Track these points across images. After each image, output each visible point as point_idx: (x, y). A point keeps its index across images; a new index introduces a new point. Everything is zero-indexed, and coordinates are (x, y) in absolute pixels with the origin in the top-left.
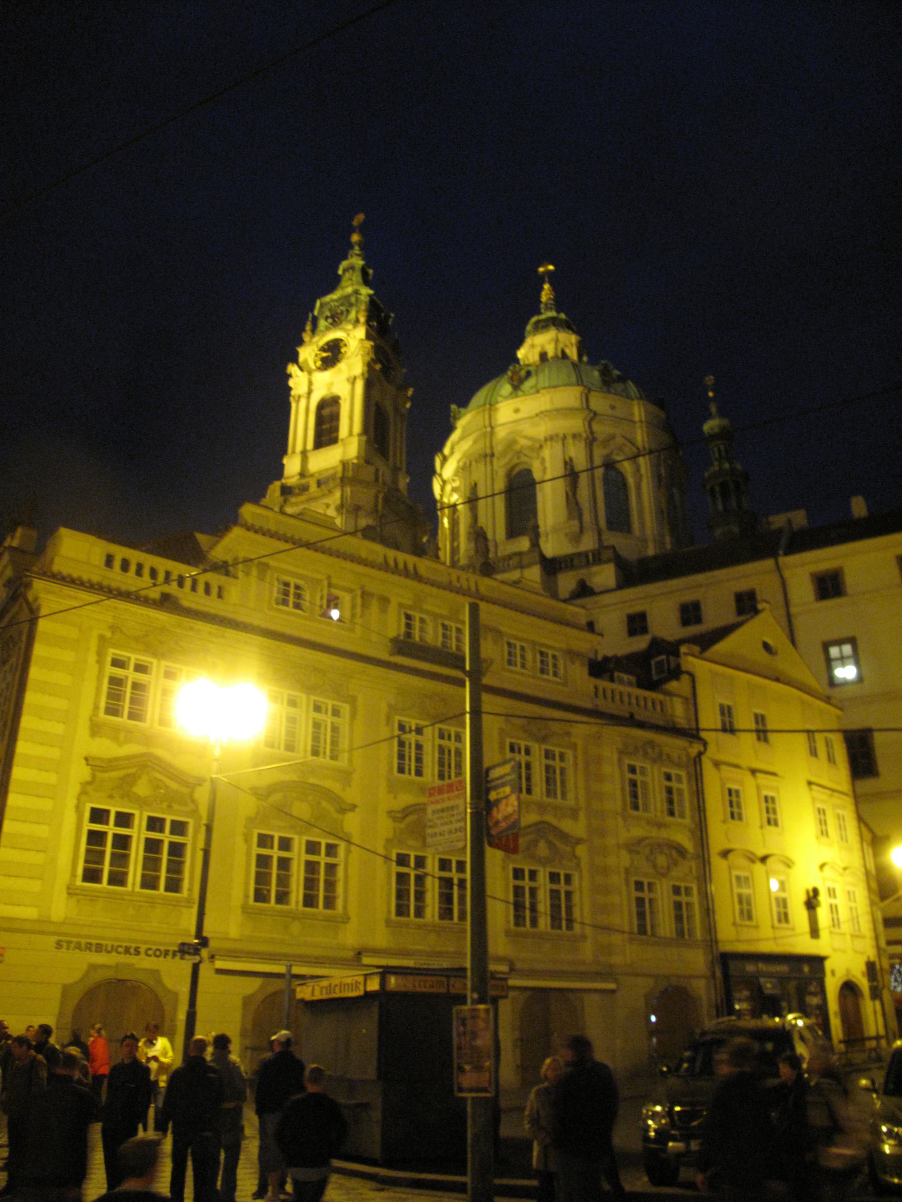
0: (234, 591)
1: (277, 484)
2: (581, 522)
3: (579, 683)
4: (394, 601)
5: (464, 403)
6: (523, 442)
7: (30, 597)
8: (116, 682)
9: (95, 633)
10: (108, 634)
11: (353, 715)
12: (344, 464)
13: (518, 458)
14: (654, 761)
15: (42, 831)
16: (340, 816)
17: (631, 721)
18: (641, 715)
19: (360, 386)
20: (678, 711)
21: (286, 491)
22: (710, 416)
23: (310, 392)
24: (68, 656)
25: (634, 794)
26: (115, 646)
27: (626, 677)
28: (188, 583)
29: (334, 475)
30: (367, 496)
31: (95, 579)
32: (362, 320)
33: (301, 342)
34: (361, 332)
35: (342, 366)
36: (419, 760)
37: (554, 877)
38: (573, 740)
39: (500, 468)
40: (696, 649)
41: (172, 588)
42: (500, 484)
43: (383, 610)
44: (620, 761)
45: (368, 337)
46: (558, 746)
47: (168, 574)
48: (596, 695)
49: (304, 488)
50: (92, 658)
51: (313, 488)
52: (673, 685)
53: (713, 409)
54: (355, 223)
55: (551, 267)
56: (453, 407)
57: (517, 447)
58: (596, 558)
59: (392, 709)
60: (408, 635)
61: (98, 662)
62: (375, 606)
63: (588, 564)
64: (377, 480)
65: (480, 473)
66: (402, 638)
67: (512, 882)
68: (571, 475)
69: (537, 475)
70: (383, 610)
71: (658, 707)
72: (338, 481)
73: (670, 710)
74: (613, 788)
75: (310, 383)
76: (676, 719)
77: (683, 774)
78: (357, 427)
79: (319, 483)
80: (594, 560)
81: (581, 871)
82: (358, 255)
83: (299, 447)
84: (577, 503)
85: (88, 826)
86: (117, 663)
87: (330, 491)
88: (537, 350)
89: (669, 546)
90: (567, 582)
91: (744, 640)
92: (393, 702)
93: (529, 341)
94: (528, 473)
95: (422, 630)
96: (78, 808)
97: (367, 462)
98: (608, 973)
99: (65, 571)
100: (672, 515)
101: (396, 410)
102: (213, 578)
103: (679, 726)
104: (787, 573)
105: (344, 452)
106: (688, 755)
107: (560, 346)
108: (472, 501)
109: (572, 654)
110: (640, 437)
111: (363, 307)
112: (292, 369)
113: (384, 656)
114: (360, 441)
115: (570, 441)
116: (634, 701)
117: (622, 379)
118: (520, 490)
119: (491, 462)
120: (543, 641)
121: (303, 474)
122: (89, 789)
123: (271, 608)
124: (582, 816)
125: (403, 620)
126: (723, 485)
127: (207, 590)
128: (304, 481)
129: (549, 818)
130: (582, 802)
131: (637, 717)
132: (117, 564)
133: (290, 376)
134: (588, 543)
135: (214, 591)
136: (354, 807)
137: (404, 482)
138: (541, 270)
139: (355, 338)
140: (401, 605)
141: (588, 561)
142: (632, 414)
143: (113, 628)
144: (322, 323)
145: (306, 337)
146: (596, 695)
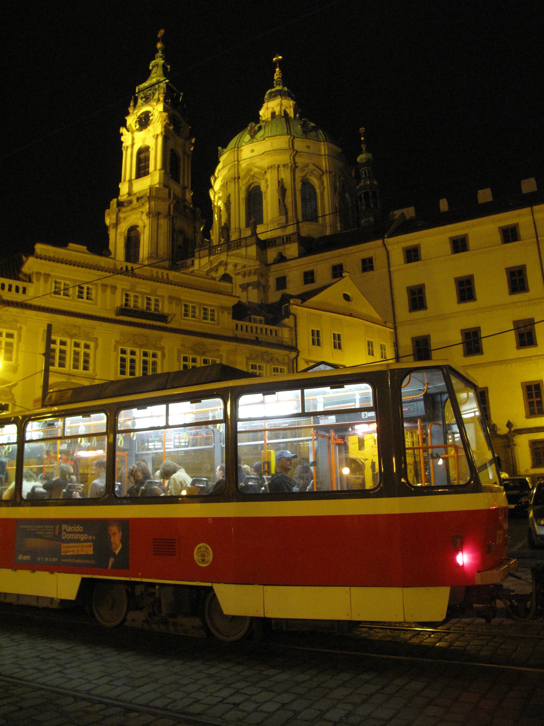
0: (32, 290)
1: (115, 200)
2: (287, 217)
3: (227, 322)
4: (120, 287)
5: (225, 146)
6: (256, 170)
12: (151, 188)
13: (253, 179)
14: (268, 362)
17: (257, 342)
18: (263, 338)
19: (160, 139)
20: (285, 334)
21: (120, 204)
22: (360, 152)
23: (133, 145)
27: (258, 318)
29: (146, 194)
30: (163, 207)
32: (162, 99)
33: (128, 114)
34: (160, 107)
35: (150, 128)
38: (220, 353)
39: (243, 184)
40: (299, 301)
42: (243, 195)
44: (247, 363)
45: (165, 110)
48: (237, 329)
49: (130, 202)
51: (135, 202)
52: (286, 321)
53: (364, 147)
54: (159, 36)
55: (280, 57)
56: (219, 148)
57: (252, 173)
58: (288, 239)
59: (117, 342)
60: (126, 305)
62: (109, 290)
63: (283, 243)
64: (170, 197)
65: (232, 189)
66: (123, 307)
68: (282, 190)
69: (263, 189)
72: (147, 199)
73: (280, 335)
75: (133, 139)
76: (284, 340)
78: (159, 166)
79: (138, 199)
80: (287, 241)
82: (161, 57)
83: (128, 178)
84: (285, 206)
87: (143, 204)
88: (270, 111)
89: (339, 229)
90: (272, 254)
91: (332, 295)
92: (118, 340)
93: (265, 105)
94: (258, 187)
95: (136, 301)
97: (165, 186)
100: (342, 211)
101: (184, 153)
103: (285, 344)
104: (389, 248)
105: (152, 180)
106: (289, 357)
107: (283, 108)
108: (228, 204)
109: (223, 308)
110: (324, 163)
111: (162, 91)
112: (123, 130)
113: (113, 316)
114: (160, 174)
115: (282, 168)
116: (259, 331)
117: (314, 129)
118: (254, 197)
119: (238, 182)
120: (204, 302)
121: (130, 194)
125: (124, 297)
126: (366, 194)
128: (130, 198)
131: (260, 339)
133: (122, 134)
134: (290, 230)
137: (189, 195)
138: (274, 59)
139: (157, 110)
140: (123, 290)
141: (284, 242)
142: (320, 150)
144: (140, 101)
145: (131, 110)
146: (237, 329)
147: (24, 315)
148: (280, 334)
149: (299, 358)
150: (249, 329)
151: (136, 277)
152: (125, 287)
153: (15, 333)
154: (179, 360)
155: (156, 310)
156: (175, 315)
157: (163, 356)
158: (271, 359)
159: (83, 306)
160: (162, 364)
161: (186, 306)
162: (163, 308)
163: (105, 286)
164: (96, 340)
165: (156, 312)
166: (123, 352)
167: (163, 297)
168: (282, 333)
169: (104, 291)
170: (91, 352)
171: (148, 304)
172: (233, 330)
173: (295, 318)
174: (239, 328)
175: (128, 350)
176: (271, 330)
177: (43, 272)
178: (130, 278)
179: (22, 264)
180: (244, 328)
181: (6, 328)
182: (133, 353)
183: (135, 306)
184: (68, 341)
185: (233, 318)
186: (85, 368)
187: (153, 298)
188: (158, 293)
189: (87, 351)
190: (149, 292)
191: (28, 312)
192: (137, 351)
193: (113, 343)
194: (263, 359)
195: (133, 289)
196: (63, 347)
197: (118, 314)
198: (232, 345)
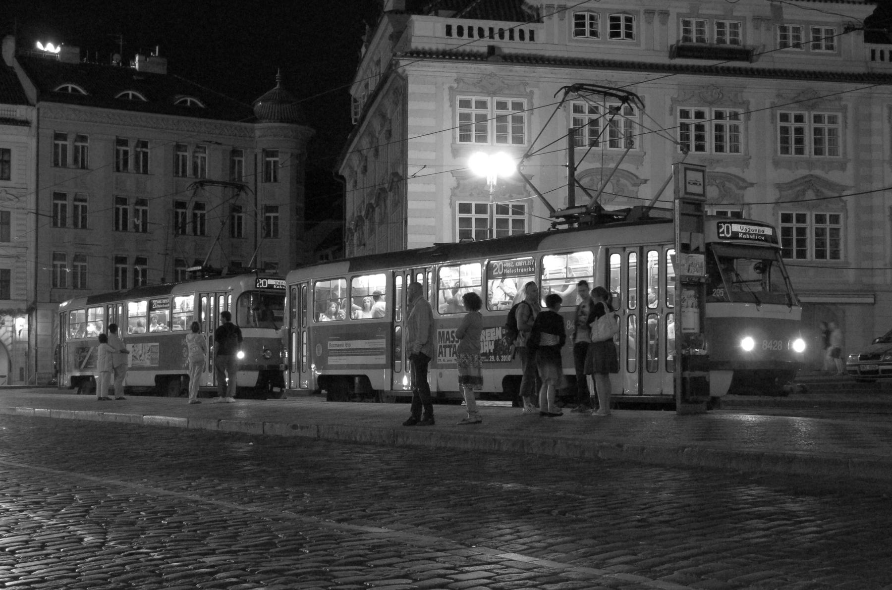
0: (541, 31)
3: (855, 50)
7: (400, 70)
8: (465, 117)
9: (446, 87)
10: (455, 85)
16: (635, 189)
24: (431, 106)
26: (462, 93)
28: (507, 34)
31: (441, 47)
36: (700, 138)
37: (820, 219)
38: (843, 103)
41: (496, 41)
43: (664, 23)
47: (491, 30)
48: (873, 58)
50: (447, 104)
60: (686, 39)
61: (451, 106)
62: (656, 19)
66: (681, 43)
70: (664, 23)
85: (458, 216)
86: (465, 104)
96: (451, 205)
98: (870, 290)
99: (420, 47)
102: (527, 27)
113: (665, 60)
123: (570, 41)
124: (850, 166)
127: (522, 37)
129: (818, 172)
130: (851, 155)
132: (454, 31)
136: (646, 181)
140: (679, 15)
143: (457, 80)
146: (873, 58)
147: (534, 74)
152: (681, 11)
153: (525, 102)
155: (734, 42)
157: (748, 113)
159: (619, 49)
160: (747, 129)
161: (784, 29)
162: (744, 35)
165: (735, 46)
166: (685, 114)
167: (745, 18)
169: (649, 22)
171: (721, 33)
172: (866, 62)
174: (878, 55)
177: (556, 4)
181: (510, 96)
182: (700, 115)
183: (701, 40)
187: (727, 23)
188: (735, 14)
190: (718, 13)
192: (706, 110)
193: (669, 102)
197: (672, 56)
198: (863, 88)
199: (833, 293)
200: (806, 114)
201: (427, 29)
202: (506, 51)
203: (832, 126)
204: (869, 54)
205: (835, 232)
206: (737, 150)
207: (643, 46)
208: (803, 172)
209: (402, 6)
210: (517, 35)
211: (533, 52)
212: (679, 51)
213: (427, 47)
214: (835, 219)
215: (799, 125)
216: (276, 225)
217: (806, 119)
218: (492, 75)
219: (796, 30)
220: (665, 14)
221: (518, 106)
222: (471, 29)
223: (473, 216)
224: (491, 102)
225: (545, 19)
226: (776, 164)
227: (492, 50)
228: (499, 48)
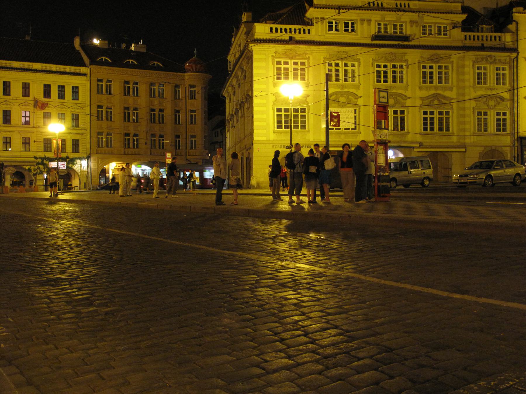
0: (313, 29)
3: (457, 36)
4: (373, 20)
7: (250, 49)
8: (279, 69)
9: (270, 56)
10: (274, 55)
11: (359, 65)
14: (491, 63)
15: (264, 116)
16: (356, 100)
17: (482, 48)
18: (487, 44)
25: (480, 79)
28: (298, 31)
31: (268, 38)
37: (441, 113)
38: (451, 60)
41: (293, 35)
43: (369, 24)
44: (473, 66)
46: (443, 63)
48: (466, 39)
50: (271, 63)
59: (374, 60)
60: (379, 32)
62: (365, 23)
67: (422, 116)
70: (369, 24)
71: (498, 39)
73: (503, 40)
74: (470, 75)
77: (507, 67)
81: (453, 110)
85: (276, 113)
86: (279, 63)
92: (374, 58)
95: (386, 29)
98: (464, 146)
99: (258, 37)
102: (307, 28)
103: (507, 47)
113: (369, 42)
116: (485, 38)
122: (275, 103)
123: (326, 33)
124: (455, 89)
127: (304, 32)
129: (438, 92)
130: (455, 83)
131: (485, 45)
132: (274, 30)
135: (307, 32)
136: (361, 97)
140: (376, 21)
143: (275, 52)
146: (466, 39)
148: (503, 39)
149: (519, 57)
150: (476, 38)
151: (384, 11)
153: (306, 61)
154: (419, 67)
156: (415, 35)
157: (407, 65)
158: (495, 60)
159: (348, 37)
161: (424, 27)
162: (406, 29)
163: (362, 20)
164: (359, 60)
166: (378, 66)
167: (406, 22)
168: (505, 38)
169: (362, 24)
170: (356, 69)
172: (462, 41)
173: (517, 23)
175: (382, 65)
176: (495, 37)
177: (320, 17)
178: (380, 12)
179: (306, 11)
180: (472, 38)
181: (300, 59)
182: (385, 66)
184: (340, 62)
185: (463, 30)
186: (353, 81)
187: (398, 24)
189: (353, 68)
190: (394, 19)
191: (313, 47)
192: (388, 64)
193: (371, 61)
194: (487, 61)
195: (383, 19)
196: (337, 68)
197: (372, 40)
198: (461, 53)
199: (447, 147)
200: (434, 65)
201: (261, 30)
202: (297, 39)
203: (446, 71)
204: (463, 37)
205: (447, 119)
206: (402, 82)
207: (359, 36)
208: (432, 92)
209: (250, 19)
210: (302, 31)
211: (310, 39)
212: (376, 37)
213: (262, 38)
214: (447, 113)
215: (431, 70)
216: (195, 119)
217: (434, 67)
218: (291, 50)
219: (430, 27)
220: (369, 20)
221: (303, 64)
222: (281, 29)
223: (283, 113)
224: (291, 62)
225: (315, 24)
226: (420, 88)
227: (291, 38)
228: (294, 38)
